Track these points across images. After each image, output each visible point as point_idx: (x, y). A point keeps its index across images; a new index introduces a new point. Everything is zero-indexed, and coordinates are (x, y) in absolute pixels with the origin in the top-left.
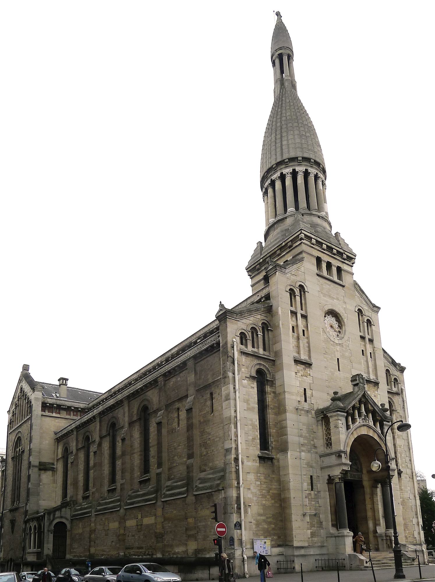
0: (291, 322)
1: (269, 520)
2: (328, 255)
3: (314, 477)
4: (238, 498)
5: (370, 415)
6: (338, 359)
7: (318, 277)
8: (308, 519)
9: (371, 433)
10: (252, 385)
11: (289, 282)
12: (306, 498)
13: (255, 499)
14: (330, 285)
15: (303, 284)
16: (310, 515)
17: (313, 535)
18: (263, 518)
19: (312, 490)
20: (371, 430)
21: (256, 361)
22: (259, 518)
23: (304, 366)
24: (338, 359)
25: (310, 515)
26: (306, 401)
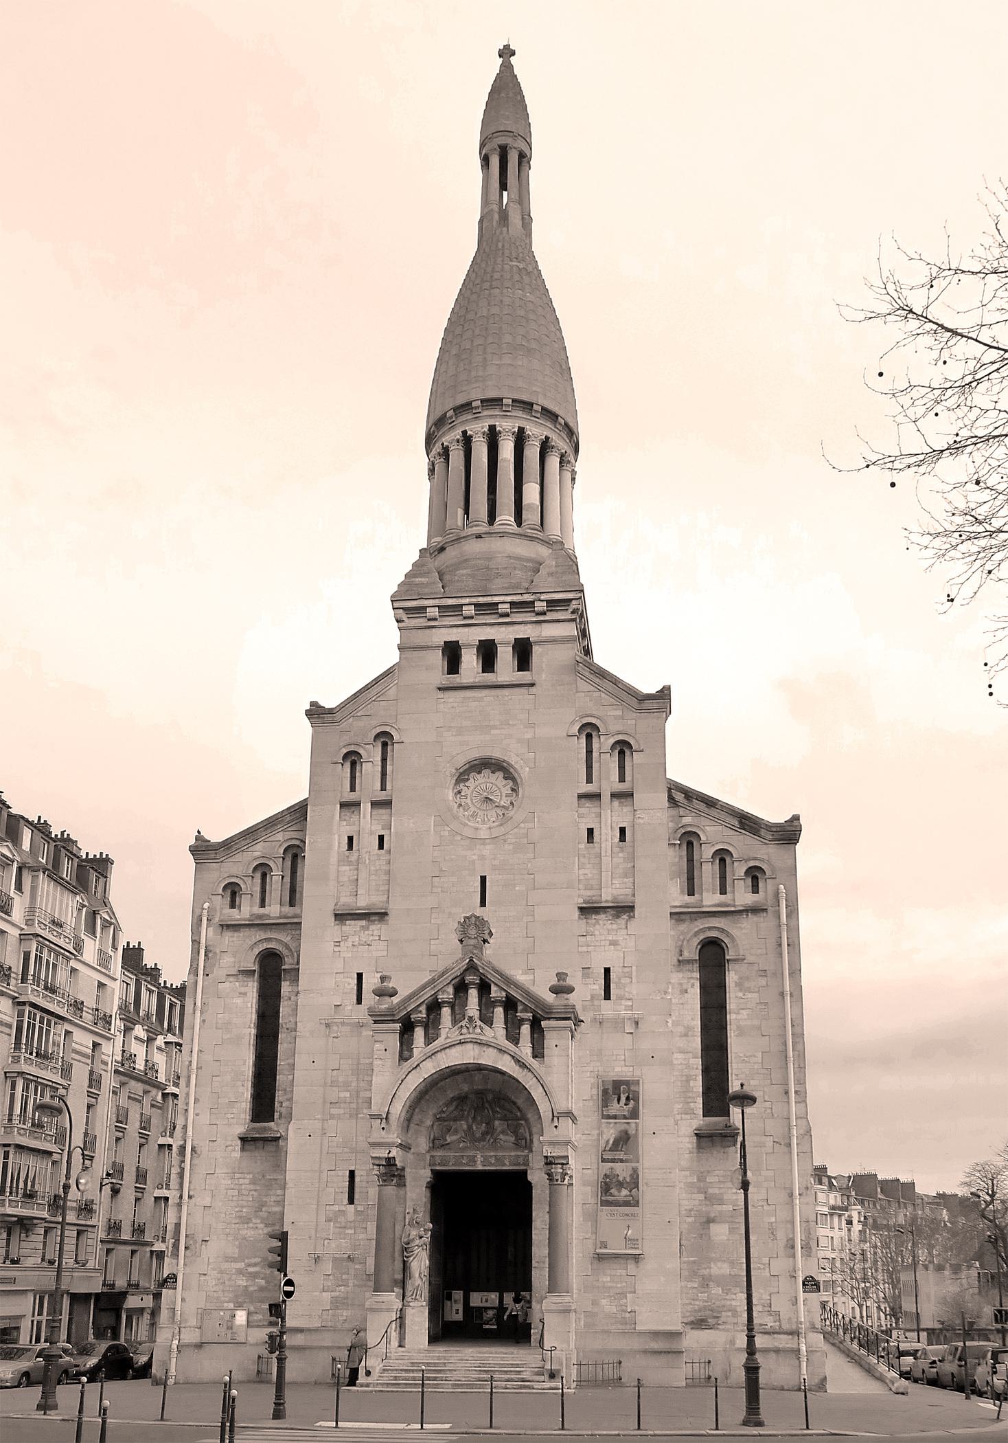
0: (341, 828)
1: (251, 1269)
2: (485, 624)
3: (357, 1173)
4: (178, 1226)
5: (499, 1012)
6: (483, 879)
7: (440, 695)
8: (328, 1267)
9: (488, 1058)
10: (243, 990)
11: (346, 739)
12: (328, 1220)
13: (220, 1226)
14: (480, 700)
15: (387, 729)
16: (335, 1259)
17: (337, 1304)
18: (241, 1265)
19: (351, 1201)
20: (491, 1049)
21: (260, 935)
22: (226, 1266)
23: (363, 923)
24: (483, 879)
25: (335, 1259)
26: (359, 1001)
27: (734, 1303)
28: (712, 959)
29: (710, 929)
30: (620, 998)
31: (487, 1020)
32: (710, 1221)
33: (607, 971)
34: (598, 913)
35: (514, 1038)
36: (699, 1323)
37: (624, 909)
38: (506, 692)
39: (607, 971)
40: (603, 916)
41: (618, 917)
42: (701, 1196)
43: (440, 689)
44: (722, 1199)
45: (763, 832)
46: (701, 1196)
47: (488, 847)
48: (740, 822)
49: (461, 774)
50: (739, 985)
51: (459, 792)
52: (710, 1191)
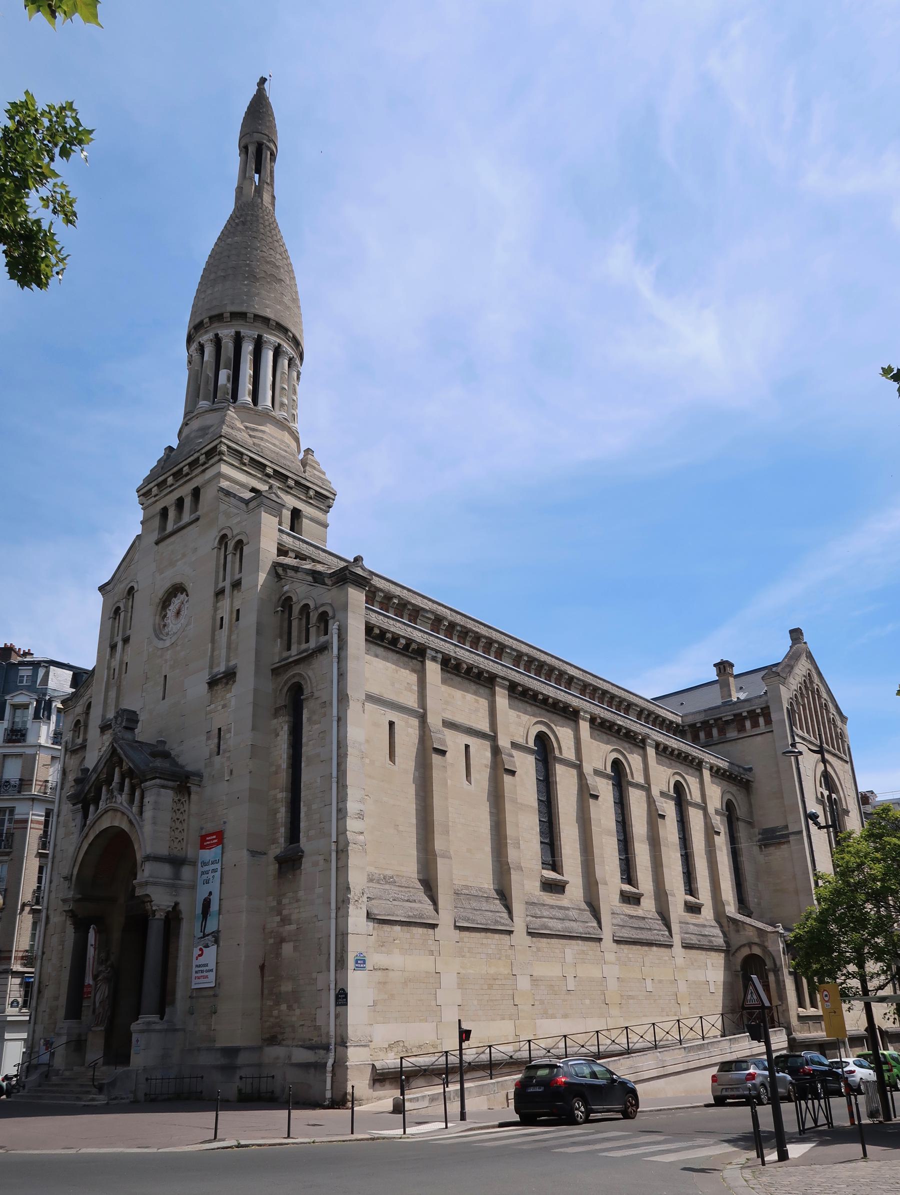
27: (294, 1019)
28: (295, 702)
29: (294, 676)
30: (225, 751)
31: (121, 790)
32: (282, 940)
33: (220, 729)
34: (217, 685)
35: (131, 801)
36: (273, 1040)
37: (230, 676)
38: (185, 531)
39: (220, 729)
40: (220, 687)
41: (227, 683)
42: (278, 919)
43: (157, 543)
44: (290, 920)
45: (327, 581)
46: (278, 919)
47: (169, 652)
48: (313, 577)
49: (164, 602)
50: (309, 719)
51: (165, 616)
52: (285, 912)
